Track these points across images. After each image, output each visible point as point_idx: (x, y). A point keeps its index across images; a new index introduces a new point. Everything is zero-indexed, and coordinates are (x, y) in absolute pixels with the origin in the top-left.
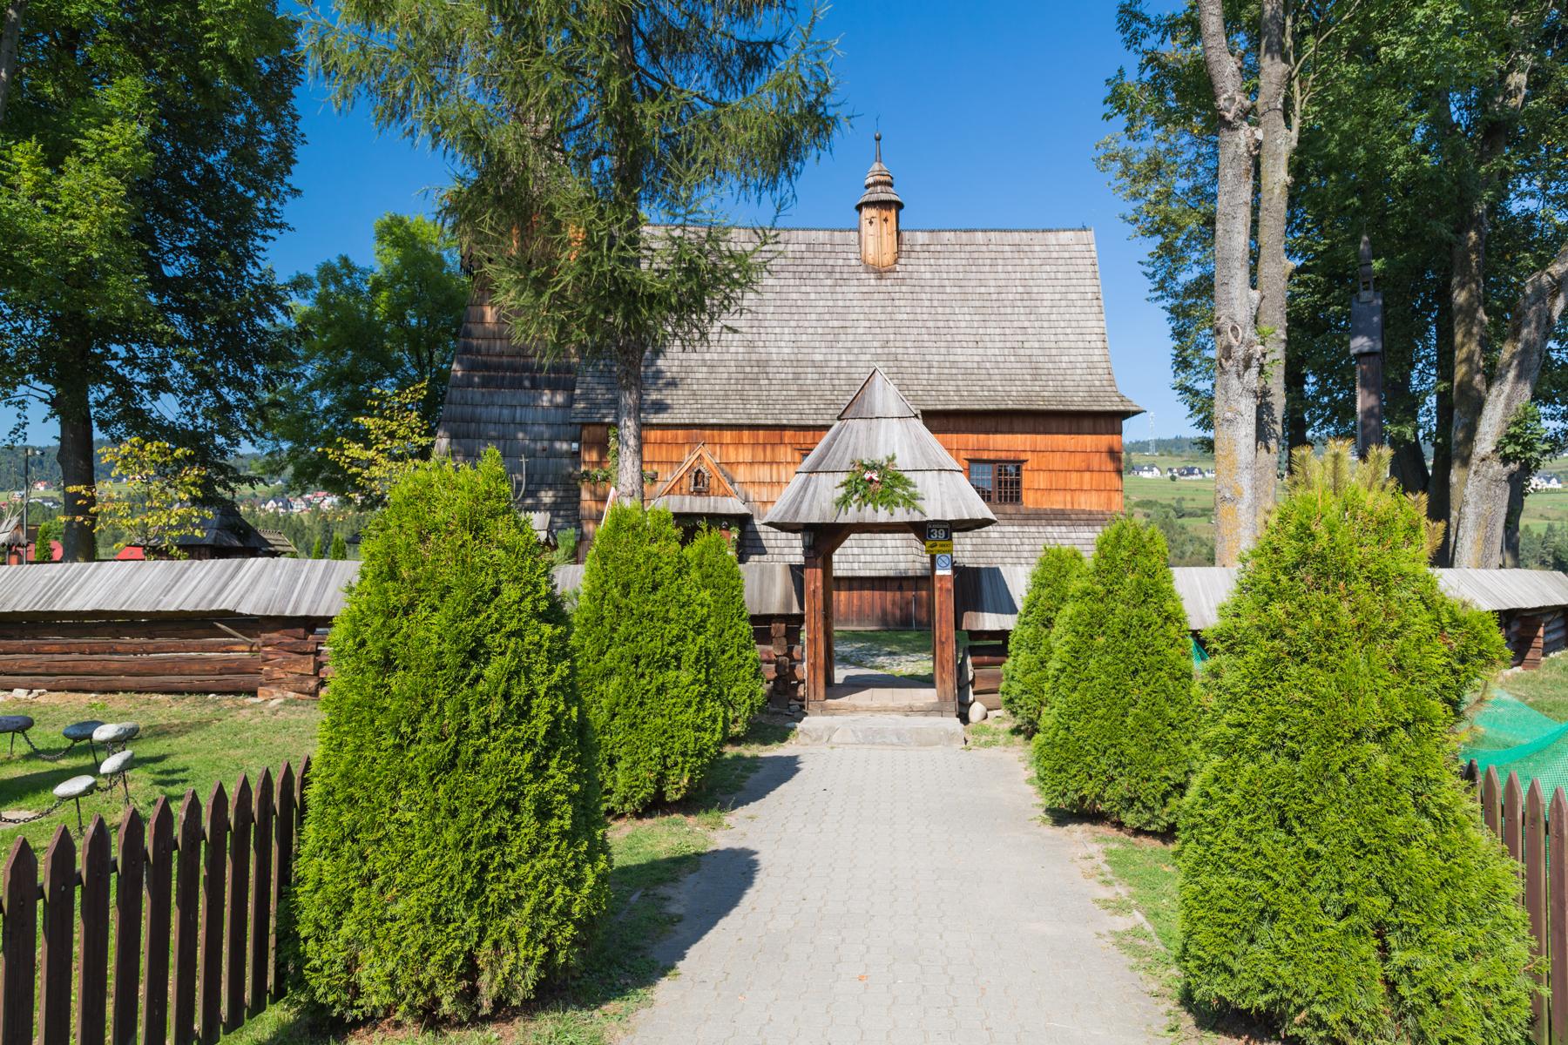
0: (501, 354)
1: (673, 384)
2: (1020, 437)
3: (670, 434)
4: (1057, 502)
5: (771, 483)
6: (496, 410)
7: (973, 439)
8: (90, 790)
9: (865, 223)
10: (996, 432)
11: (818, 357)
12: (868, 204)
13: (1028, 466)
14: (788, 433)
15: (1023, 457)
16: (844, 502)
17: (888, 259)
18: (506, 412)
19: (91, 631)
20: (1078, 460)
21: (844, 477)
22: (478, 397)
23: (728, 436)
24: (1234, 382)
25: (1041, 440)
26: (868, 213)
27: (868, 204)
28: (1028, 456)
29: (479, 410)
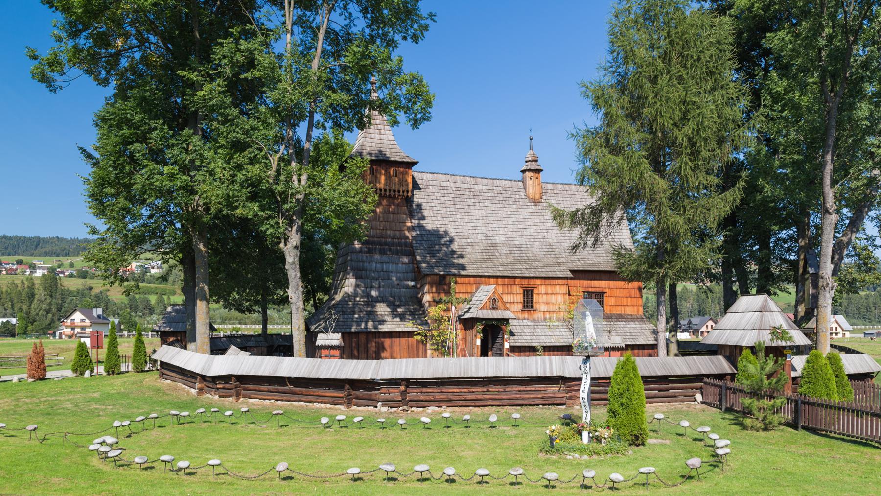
0: (374, 237)
1: (461, 256)
2: (603, 282)
3: (467, 279)
4: (618, 311)
5: (511, 303)
6: (374, 265)
7: (586, 283)
8: (161, 455)
9: (528, 179)
10: (594, 279)
11: (517, 243)
12: (530, 170)
13: (607, 295)
14: (517, 280)
15: (605, 291)
16: (772, 340)
17: (538, 196)
18: (379, 266)
19: (187, 375)
20: (626, 293)
21: (769, 332)
22: (365, 258)
23: (492, 280)
24: (828, 294)
25: (612, 283)
26: (528, 174)
27: (530, 170)
28: (606, 290)
29: (366, 265)
